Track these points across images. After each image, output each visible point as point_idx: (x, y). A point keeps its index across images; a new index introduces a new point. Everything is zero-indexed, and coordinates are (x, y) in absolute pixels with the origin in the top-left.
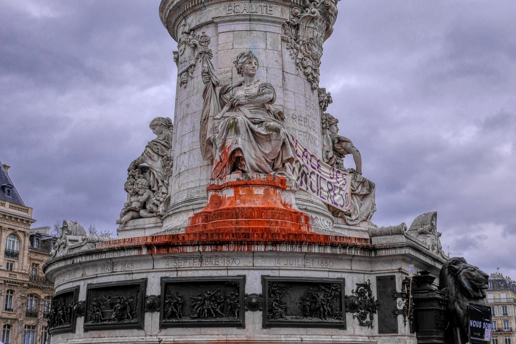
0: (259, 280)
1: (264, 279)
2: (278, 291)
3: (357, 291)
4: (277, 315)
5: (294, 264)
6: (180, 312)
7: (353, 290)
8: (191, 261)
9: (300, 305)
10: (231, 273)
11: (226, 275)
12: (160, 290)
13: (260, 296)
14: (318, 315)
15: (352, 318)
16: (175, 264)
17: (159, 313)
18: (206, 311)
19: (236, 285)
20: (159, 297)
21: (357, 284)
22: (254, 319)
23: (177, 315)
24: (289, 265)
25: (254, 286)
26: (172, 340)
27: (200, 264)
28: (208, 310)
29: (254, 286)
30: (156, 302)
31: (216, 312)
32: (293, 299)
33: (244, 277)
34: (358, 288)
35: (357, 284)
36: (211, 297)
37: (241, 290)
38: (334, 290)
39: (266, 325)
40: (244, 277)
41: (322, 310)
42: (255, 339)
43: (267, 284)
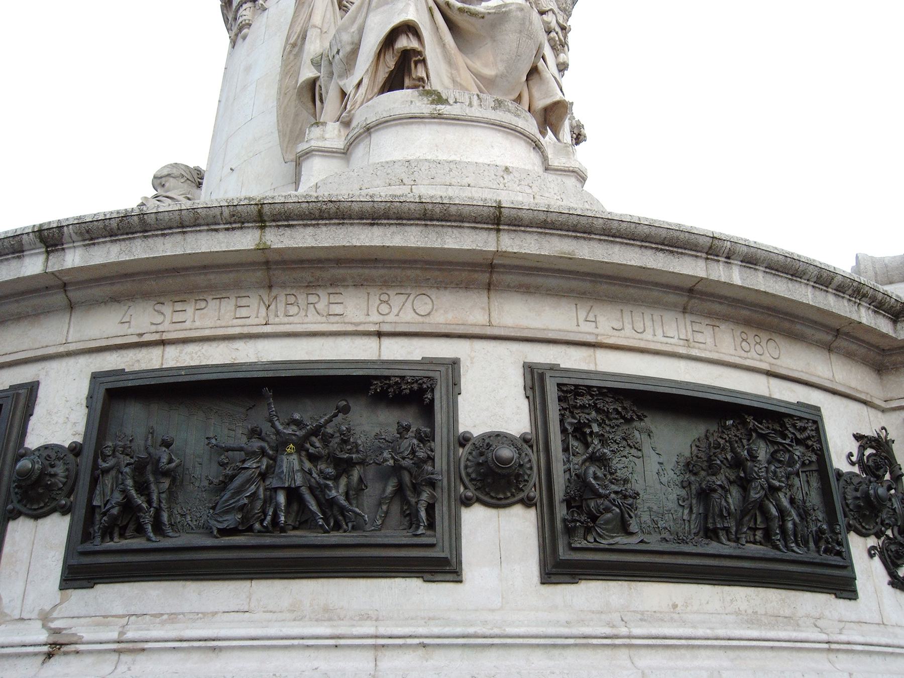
0: (516, 380)
1: (536, 378)
2: (596, 429)
3: (860, 462)
4: (607, 522)
5: (649, 330)
6: (158, 511)
7: (851, 454)
8: (224, 302)
9: (683, 493)
10: (395, 351)
11: (375, 358)
12: (81, 428)
13: (525, 439)
14: (759, 535)
15: (866, 555)
16: (159, 319)
17: (67, 519)
18: (281, 498)
19: (422, 391)
20: (76, 450)
21: (858, 437)
22: (499, 540)
23: (147, 520)
24: (628, 331)
25: (492, 402)
26: (114, 635)
27: (263, 310)
28: (293, 494)
29: (492, 402)
30: (60, 470)
31: (328, 505)
32: (655, 465)
33: (454, 364)
34: (862, 448)
35: (858, 437)
36: (306, 438)
37: (440, 416)
38: (799, 442)
39: (557, 569)
40: (454, 364)
41: (774, 511)
42: (510, 630)
43: (552, 393)
